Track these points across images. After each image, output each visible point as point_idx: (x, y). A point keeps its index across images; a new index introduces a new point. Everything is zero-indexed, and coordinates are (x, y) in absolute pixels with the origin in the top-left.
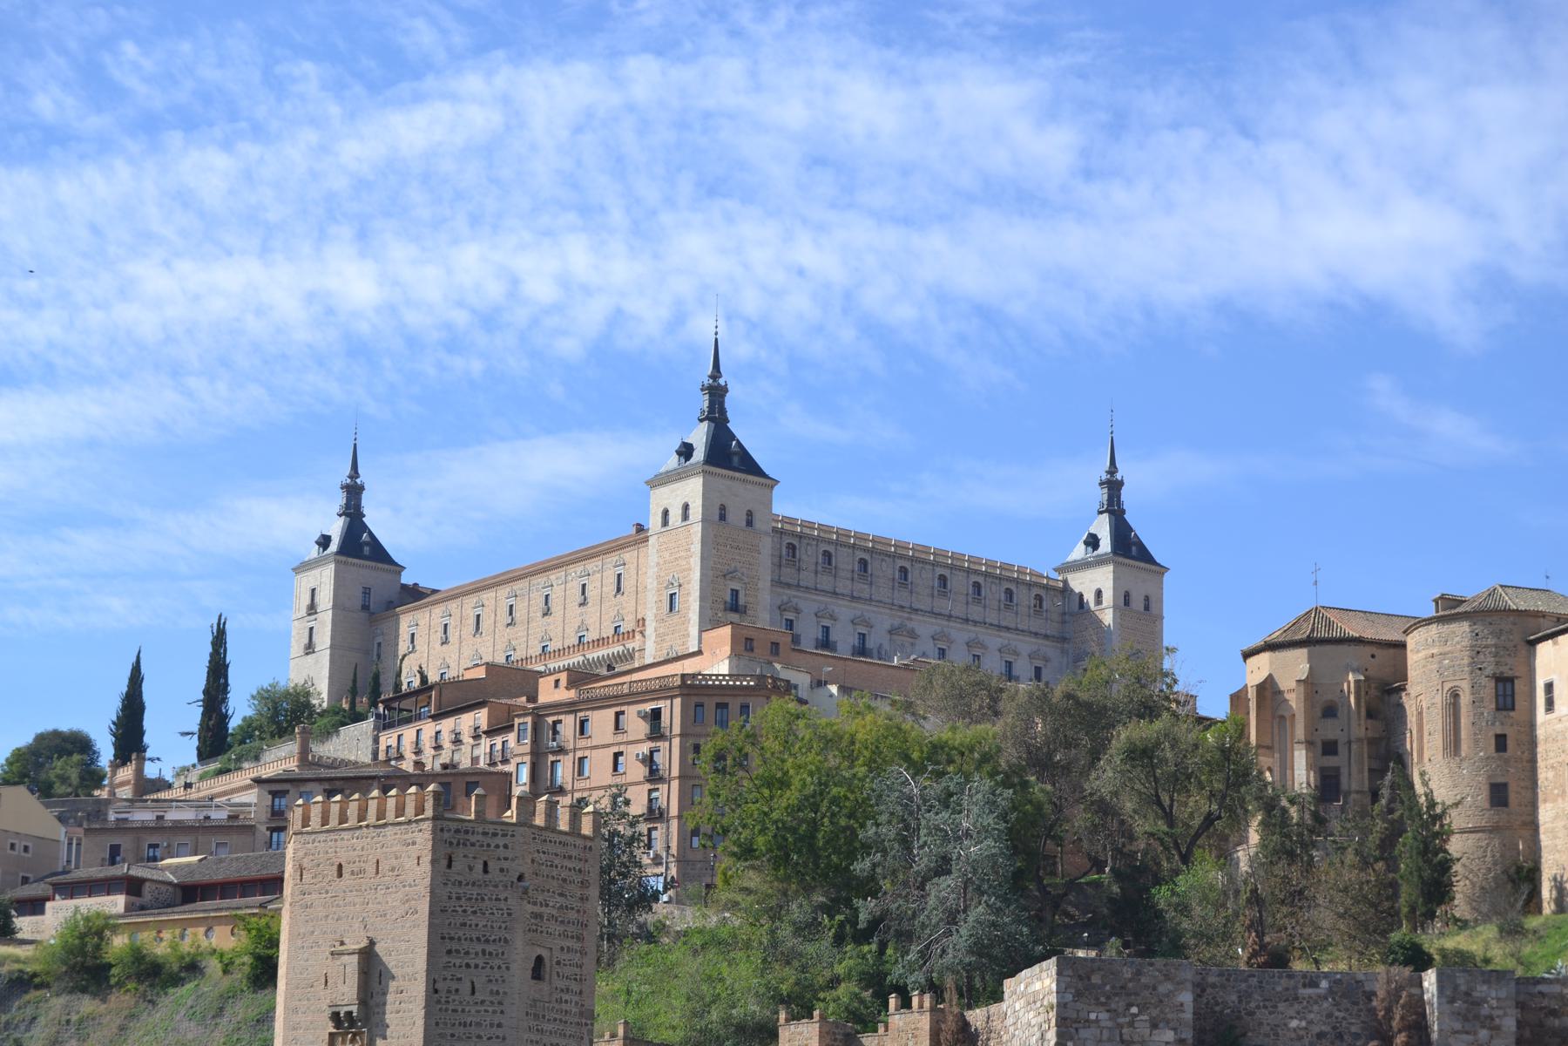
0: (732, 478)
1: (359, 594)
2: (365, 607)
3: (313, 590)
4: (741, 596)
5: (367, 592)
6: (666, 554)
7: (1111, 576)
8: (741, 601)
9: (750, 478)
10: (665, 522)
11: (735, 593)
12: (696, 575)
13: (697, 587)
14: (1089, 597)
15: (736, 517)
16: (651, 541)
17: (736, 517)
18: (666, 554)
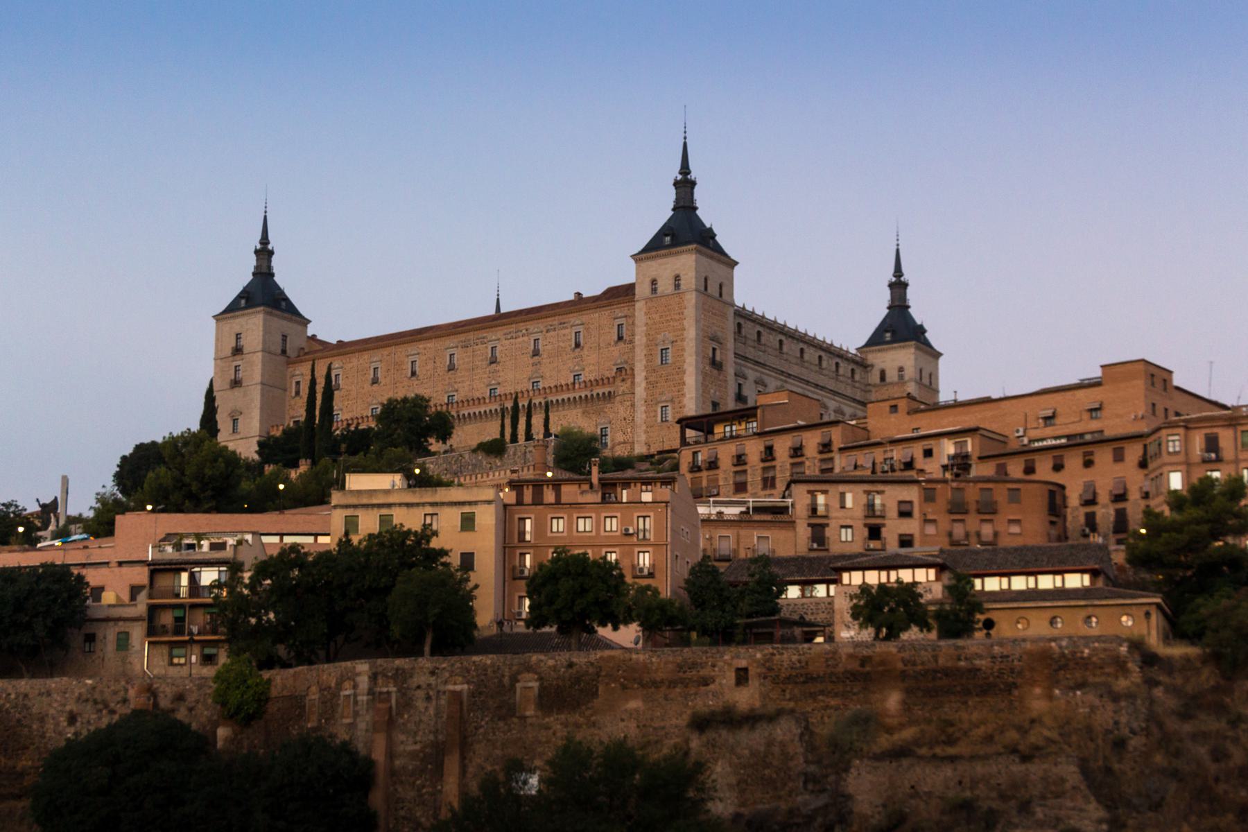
0: (712, 258)
1: (279, 338)
2: (284, 352)
3: (238, 337)
4: (718, 352)
5: (284, 337)
6: (657, 317)
7: (912, 357)
8: (718, 358)
9: (716, 254)
10: (654, 290)
11: (714, 349)
12: (691, 333)
13: (693, 344)
14: (892, 376)
15: (713, 289)
16: (639, 305)
17: (713, 289)
18: (657, 317)
